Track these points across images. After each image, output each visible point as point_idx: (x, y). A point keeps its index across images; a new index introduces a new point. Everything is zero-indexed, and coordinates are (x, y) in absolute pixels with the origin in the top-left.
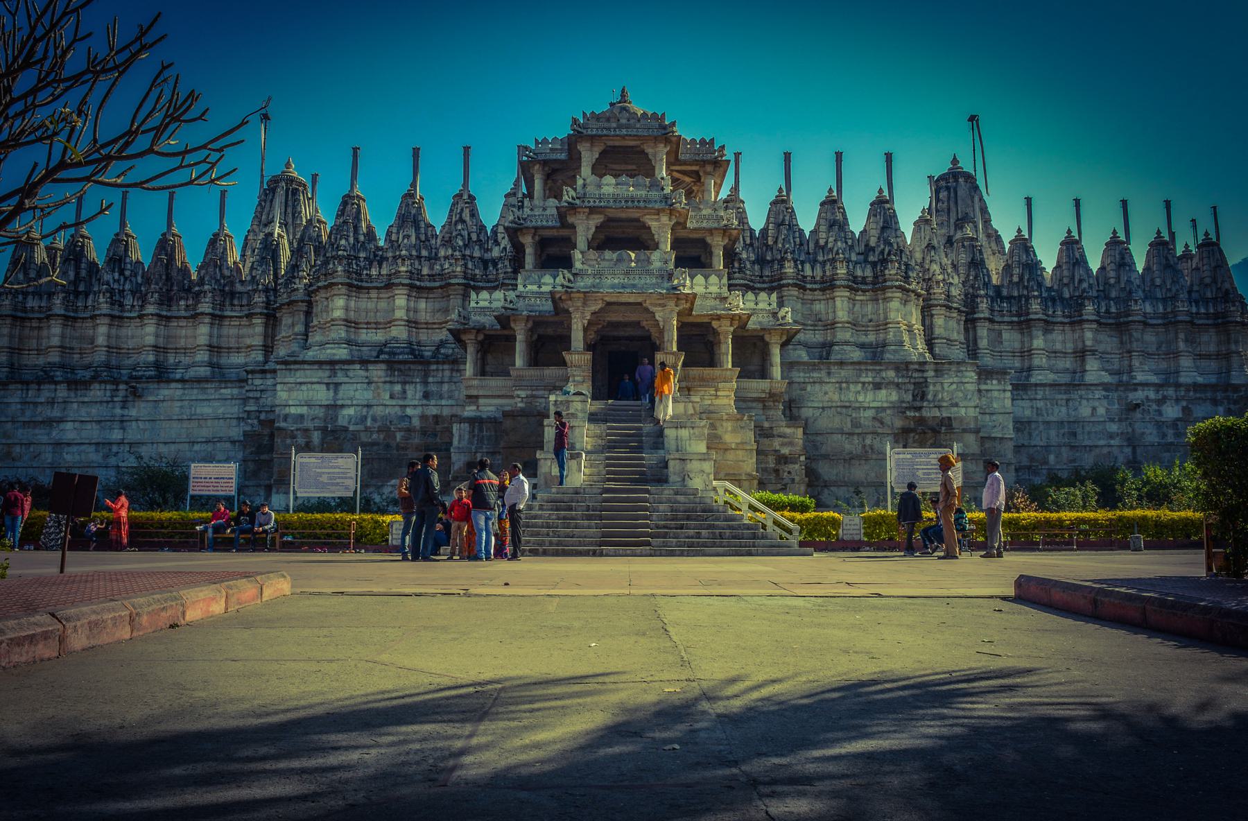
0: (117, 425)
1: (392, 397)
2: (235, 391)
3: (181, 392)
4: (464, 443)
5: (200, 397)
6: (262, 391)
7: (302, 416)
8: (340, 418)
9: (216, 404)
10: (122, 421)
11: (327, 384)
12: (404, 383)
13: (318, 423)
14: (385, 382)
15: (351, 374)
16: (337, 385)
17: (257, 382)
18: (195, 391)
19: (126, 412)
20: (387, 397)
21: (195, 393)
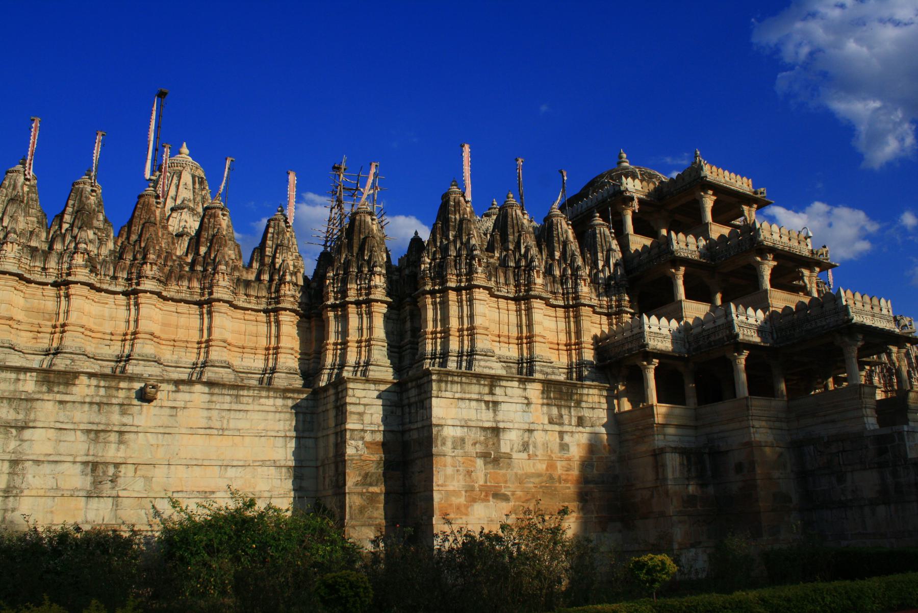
0: (113, 437)
1: (551, 422)
2: (279, 402)
3: (207, 398)
4: (677, 475)
5: (235, 407)
6: (365, 405)
7: (463, 440)
8: (502, 442)
9: (256, 416)
10: (121, 433)
11: (487, 403)
12: (559, 407)
13: (479, 448)
14: (543, 404)
15: (509, 391)
16: (496, 403)
17: (359, 393)
18: (228, 399)
19: (126, 420)
20: (546, 421)
21: (225, 400)
